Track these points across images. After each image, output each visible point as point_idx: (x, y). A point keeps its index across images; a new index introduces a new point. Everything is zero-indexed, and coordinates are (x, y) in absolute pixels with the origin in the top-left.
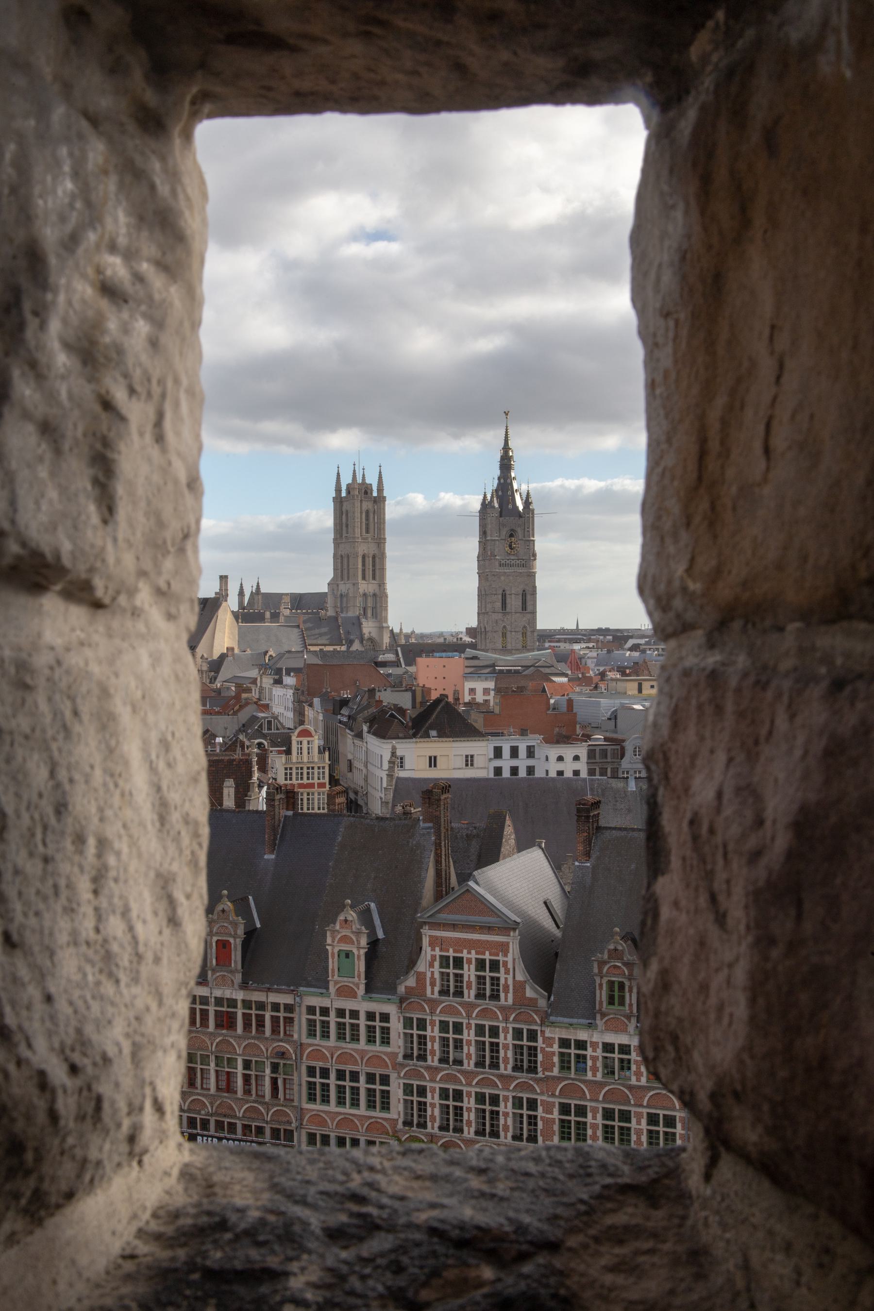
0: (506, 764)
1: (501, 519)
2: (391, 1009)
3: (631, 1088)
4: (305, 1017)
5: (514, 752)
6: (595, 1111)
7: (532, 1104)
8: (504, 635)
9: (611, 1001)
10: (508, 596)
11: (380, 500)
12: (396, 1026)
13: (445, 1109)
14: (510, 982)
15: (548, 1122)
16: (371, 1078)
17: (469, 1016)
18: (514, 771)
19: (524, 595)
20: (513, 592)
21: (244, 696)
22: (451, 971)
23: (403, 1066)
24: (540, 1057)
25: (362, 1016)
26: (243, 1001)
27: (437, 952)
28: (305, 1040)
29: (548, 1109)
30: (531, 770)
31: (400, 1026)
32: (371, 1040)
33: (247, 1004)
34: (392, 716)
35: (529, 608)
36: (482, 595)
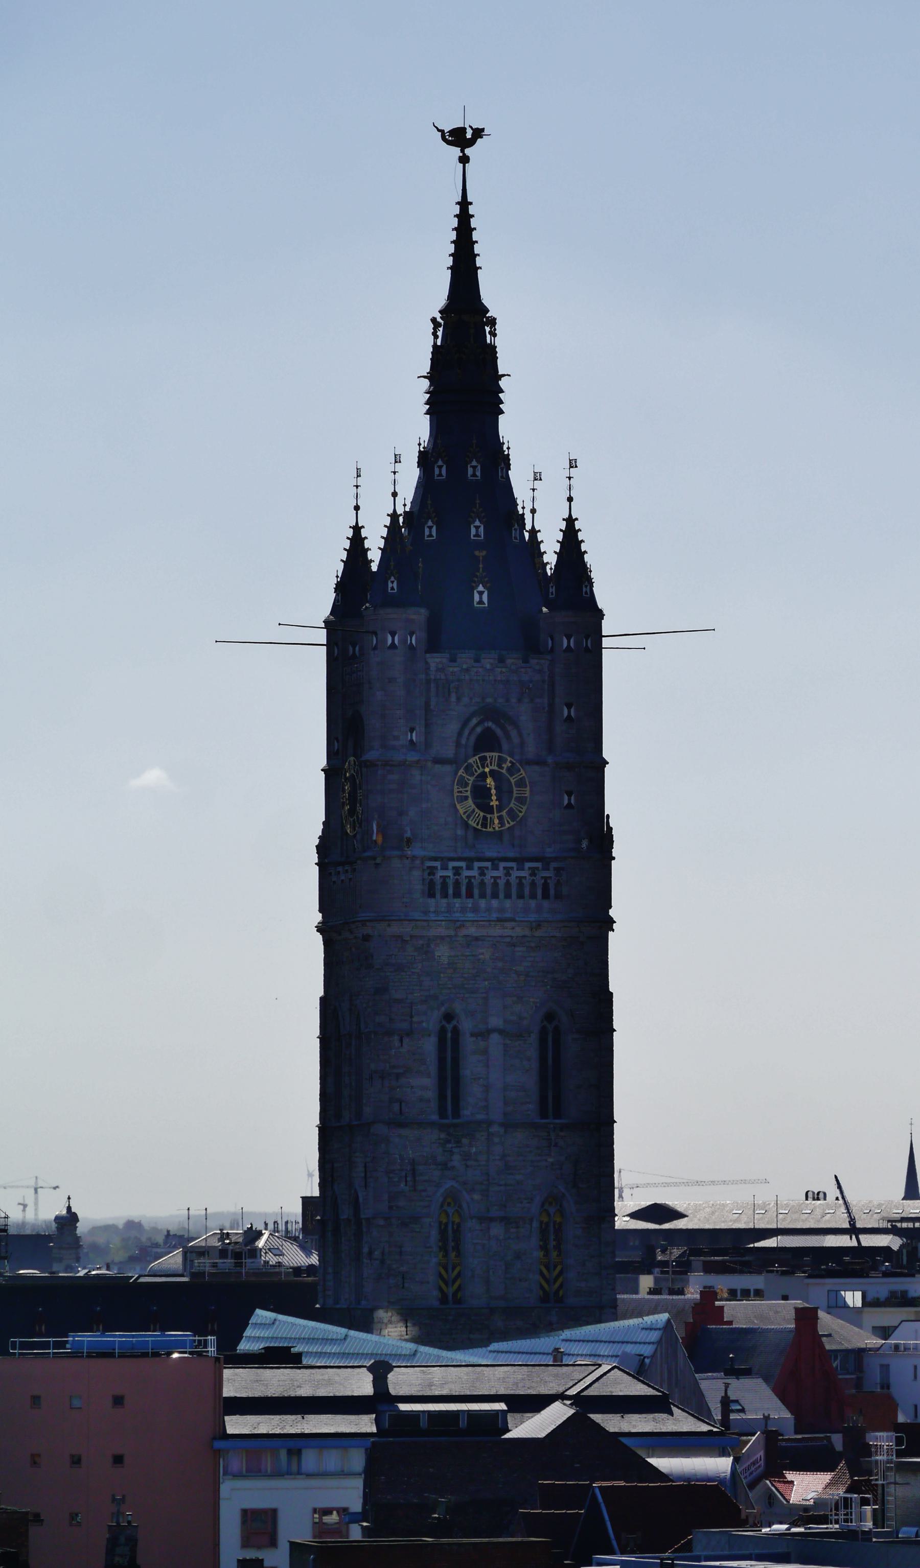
1: (435, 660)
10: (468, 1043)
20: (495, 1021)
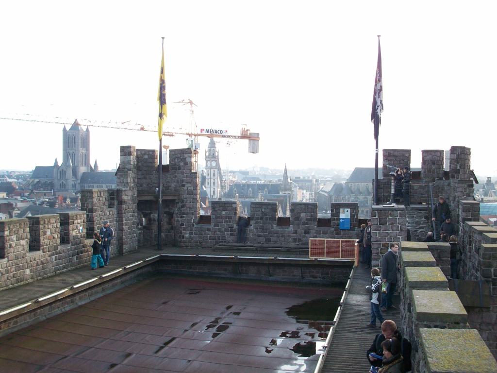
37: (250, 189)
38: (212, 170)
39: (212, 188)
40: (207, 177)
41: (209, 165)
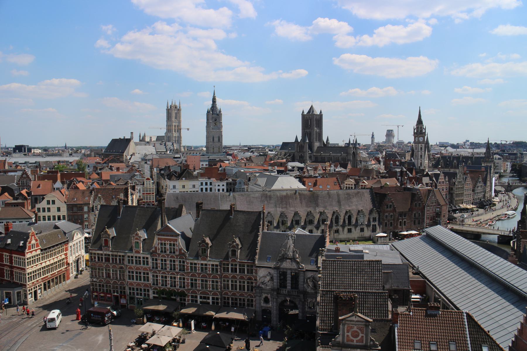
0: (204, 187)
2: (149, 256)
3: (207, 274)
4: (127, 258)
5: (206, 184)
6: (199, 280)
7: (184, 279)
8: (213, 149)
9: (202, 253)
11: (179, 110)
12: (150, 260)
13: (162, 281)
14: (178, 249)
15: (188, 283)
16: (144, 273)
17: (168, 257)
18: (206, 189)
19: (219, 137)
21: (133, 168)
22: (163, 246)
23: (152, 270)
24: (185, 267)
25: (142, 258)
26: (112, 255)
27: (160, 242)
28: (127, 264)
29: (188, 280)
30: (211, 189)
31: (151, 260)
32: (144, 264)
33: (112, 255)
34: (173, 174)
35: (220, 141)
36: (207, 137)
37: (455, 161)
38: (420, 145)
39: (419, 160)
40: (415, 151)
41: (417, 140)
